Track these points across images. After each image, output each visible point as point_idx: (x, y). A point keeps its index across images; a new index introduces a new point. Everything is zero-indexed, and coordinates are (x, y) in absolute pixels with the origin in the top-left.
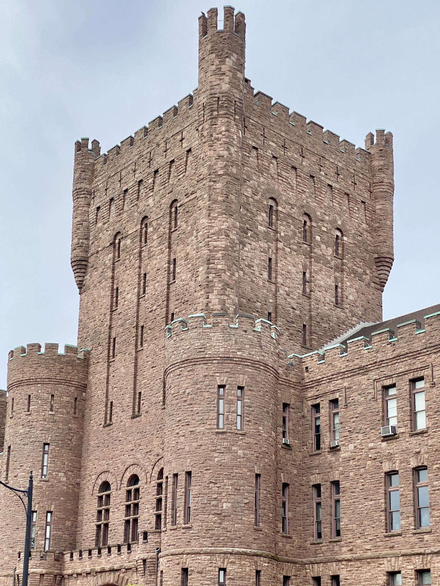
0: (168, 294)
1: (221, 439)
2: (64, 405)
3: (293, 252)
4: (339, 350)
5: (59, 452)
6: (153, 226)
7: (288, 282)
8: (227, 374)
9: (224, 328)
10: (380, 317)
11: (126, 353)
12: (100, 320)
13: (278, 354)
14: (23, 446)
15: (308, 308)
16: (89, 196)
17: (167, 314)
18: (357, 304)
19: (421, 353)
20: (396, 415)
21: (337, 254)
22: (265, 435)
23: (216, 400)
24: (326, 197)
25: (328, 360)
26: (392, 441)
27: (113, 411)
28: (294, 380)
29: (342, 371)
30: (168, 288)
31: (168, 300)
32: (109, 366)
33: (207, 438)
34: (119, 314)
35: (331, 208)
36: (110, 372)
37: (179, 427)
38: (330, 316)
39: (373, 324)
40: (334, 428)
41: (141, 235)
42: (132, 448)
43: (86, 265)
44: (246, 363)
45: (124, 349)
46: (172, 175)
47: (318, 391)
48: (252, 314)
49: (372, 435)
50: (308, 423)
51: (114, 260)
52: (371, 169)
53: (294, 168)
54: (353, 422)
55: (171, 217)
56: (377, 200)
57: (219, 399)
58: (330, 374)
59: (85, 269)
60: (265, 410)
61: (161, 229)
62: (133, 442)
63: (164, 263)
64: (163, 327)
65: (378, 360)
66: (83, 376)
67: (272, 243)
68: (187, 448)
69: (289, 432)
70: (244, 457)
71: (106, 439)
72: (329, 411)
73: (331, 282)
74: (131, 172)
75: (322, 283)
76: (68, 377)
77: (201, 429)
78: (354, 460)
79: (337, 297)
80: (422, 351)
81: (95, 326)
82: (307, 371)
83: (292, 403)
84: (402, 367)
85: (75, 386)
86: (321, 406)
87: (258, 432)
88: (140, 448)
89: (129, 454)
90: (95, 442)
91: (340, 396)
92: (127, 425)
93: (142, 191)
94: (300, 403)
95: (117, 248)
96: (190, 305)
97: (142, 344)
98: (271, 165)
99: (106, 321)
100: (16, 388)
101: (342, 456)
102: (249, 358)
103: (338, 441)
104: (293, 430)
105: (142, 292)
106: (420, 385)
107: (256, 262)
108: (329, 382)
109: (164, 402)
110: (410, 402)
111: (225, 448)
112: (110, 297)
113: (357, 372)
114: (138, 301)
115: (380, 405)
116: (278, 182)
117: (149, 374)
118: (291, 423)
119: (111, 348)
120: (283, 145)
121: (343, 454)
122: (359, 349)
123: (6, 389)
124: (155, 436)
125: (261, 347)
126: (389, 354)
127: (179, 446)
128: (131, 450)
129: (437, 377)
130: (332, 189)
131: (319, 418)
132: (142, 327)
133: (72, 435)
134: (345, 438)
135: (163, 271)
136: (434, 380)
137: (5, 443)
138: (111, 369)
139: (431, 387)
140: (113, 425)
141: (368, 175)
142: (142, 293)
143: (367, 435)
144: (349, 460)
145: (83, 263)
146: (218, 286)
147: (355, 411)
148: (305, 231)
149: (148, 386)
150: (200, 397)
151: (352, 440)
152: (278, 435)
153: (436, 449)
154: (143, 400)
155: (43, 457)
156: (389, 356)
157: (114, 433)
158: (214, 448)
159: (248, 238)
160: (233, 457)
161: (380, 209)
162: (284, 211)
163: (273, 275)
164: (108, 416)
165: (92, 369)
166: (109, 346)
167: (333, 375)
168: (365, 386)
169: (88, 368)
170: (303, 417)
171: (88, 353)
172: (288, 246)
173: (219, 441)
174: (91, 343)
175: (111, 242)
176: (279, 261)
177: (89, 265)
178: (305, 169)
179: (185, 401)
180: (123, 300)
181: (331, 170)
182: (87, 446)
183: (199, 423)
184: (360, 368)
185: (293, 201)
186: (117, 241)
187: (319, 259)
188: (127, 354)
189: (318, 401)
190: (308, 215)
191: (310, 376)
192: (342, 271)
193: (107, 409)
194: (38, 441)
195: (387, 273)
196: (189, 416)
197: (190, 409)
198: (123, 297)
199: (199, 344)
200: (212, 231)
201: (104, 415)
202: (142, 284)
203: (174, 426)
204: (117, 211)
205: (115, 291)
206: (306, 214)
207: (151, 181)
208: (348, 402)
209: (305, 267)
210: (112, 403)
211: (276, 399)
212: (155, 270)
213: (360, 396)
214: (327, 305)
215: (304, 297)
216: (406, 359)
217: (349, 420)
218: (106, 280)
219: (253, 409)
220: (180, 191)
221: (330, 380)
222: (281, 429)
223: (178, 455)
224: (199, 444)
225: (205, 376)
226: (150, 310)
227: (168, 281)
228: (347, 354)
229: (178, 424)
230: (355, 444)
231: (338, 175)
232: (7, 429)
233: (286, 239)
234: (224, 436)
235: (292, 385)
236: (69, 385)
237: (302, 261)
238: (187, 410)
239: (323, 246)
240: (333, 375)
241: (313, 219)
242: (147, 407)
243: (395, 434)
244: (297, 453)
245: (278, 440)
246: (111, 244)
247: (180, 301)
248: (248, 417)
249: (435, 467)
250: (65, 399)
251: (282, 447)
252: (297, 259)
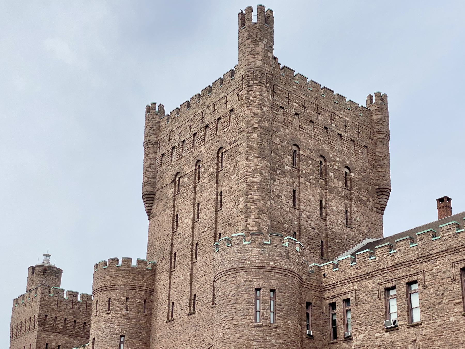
0: (216, 218)
1: (259, 331)
2: (136, 306)
3: (312, 185)
4: (350, 260)
5: (133, 342)
6: (204, 167)
7: (309, 208)
8: (263, 280)
9: (260, 244)
10: (382, 234)
11: (184, 264)
12: (164, 239)
13: (302, 264)
14: (104, 338)
15: (324, 228)
16: (156, 146)
17: (216, 233)
18: (363, 225)
19: (414, 262)
20: (396, 311)
21: (346, 186)
22: (293, 328)
23: (254, 300)
24: (336, 143)
25: (341, 268)
26: (393, 331)
27: (174, 310)
28: (315, 284)
29: (352, 276)
30: (216, 214)
31: (216, 223)
32: (171, 275)
33: (247, 330)
34: (179, 234)
35: (340, 151)
36: (172, 279)
37: (225, 321)
38: (341, 234)
39: (376, 240)
40: (347, 322)
41: (196, 174)
42: (188, 339)
43: (153, 198)
44: (277, 271)
45: (182, 261)
46: (219, 129)
47: (334, 292)
48: (281, 233)
49: (378, 327)
50: (327, 318)
51: (175, 193)
52: (372, 121)
53: (312, 122)
54: (363, 317)
55: (218, 160)
56: (376, 145)
57: (256, 299)
58: (343, 279)
59: (153, 201)
60: (293, 307)
61: (211, 169)
62: (190, 334)
63: (213, 195)
64: (212, 244)
65: (381, 268)
66: (151, 283)
67: (296, 179)
68: (232, 338)
69: (312, 326)
70: (276, 345)
71: (168, 331)
72: (343, 308)
73: (342, 208)
74: (188, 127)
75: (335, 208)
76: (140, 283)
77: (243, 323)
78: (364, 347)
79: (347, 219)
80: (415, 261)
81: (160, 244)
82: (325, 277)
83: (313, 302)
84: (400, 273)
85: (145, 290)
86: (336, 305)
87: (287, 325)
88: (195, 338)
89: (186, 344)
90: (159, 334)
91: (351, 297)
92: (185, 320)
93: (196, 141)
94: (320, 302)
95: (177, 184)
96: (233, 226)
97: (196, 257)
98: (295, 120)
99: (168, 240)
100: (99, 293)
101: (354, 343)
102: (279, 267)
103: (351, 332)
104: (315, 324)
105: (196, 218)
106: (414, 287)
107: (284, 193)
108: (342, 285)
109: (213, 302)
110: (407, 301)
111: (261, 338)
112: (172, 221)
113: (365, 278)
114: (193, 224)
115: (384, 303)
116: (300, 133)
117: (202, 280)
118: (313, 317)
119: (173, 261)
120: (303, 105)
121: (355, 343)
122: (366, 259)
123: (92, 294)
124: (206, 329)
125: (288, 258)
126: (389, 263)
127: (225, 337)
128: (188, 340)
129: (428, 280)
130: (341, 137)
131: (335, 314)
132: (197, 244)
133: (142, 329)
134: (356, 329)
135: (212, 201)
136: (426, 283)
137: (90, 336)
138: (172, 277)
139: (423, 289)
140: (174, 321)
141: (369, 126)
142: (196, 218)
143: (374, 327)
144: (360, 347)
145: (151, 196)
146: (255, 212)
147: (363, 308)
148: (321, 169)
149: (201, 289)
150: (242, 298)
151: (361, 331)
152: (303, 328)
153: (429, 338)
154: (197, 301)
155: (120, 347)
156: (390, 264)
157: (175, 327)
158: (253, 338)
159: (277, 175)
160: (268, 345)
161: (379, 152)
162: (304, 154)
163: (297, 203)
164: (170, 314)
165: (157, 277)
166: (171, 259)
167: (345, 280)
168: (371, 288)
169: (154, 277)
170: (323, 313)
171: (155, 265)
172: (308, 180)
173: (257, 332)
174: (157, 257)
175: (173, 180)
176: (301, 192)
177: (156, 198)
178: (320, 123)
179: (230, 301)
180: (182, 224)
181: (341, 123)
182: (154, 338)
183: (241, 318)
184: (367, 274)
185: (311, 147)
186: (177, 179)
187: (332, 190)
188: (185, 265)
189: (334, 300)
190: (323, 157)
191: (328, 280)
192: (350, 199)
193: (169, 308)
194: (116, 334)
195: (386, 200)
196: (233, 312)
197: (234, 308)
198: (181, 221)
199: (240, 257)
200: (250, 170)
201: (167, 313)
202: (196, 211)
203: (221, 321)
204: (177, 157)
205: (176, 217)
206: (322, 156)
207: (203, 133)
208: (358, 301)
209: (321, 196)
210: (173, 303)
211: (301, 298)
212: (206, 200)
213: (367, 296)
214: (339, 225)
215: (322, 220)
216: (403, 267)
217: (359, 315)
218: (169, 209)
219: (283, 307)
220: (225, 140)
221: (343, 284)
222: (305, 323)
223: (225, 343)
224: (241, 335)
225: (245, 281)
226: (202, 231)
227: (216, 209)
228: (356, 263)
229: (224, 319)
230: (365, 335)
231: (346, 126)
232: (92, 325)
233: (307, 176)
234: (260, 329)
235: (313, 288)
236: (140, 289)
237: (320, 192)
238: (231, 308)
239: (335, 181)
240: (345, 280)
241: (327, 160)
242: (200, 306)
243: (396, 326)
244: (318, 342)
245: (303, 331)
246: (172, 182)
247: (225, 224)
248: (279, 313)
250: (138, 301)
251: (306, 337)
252: (315, 191)
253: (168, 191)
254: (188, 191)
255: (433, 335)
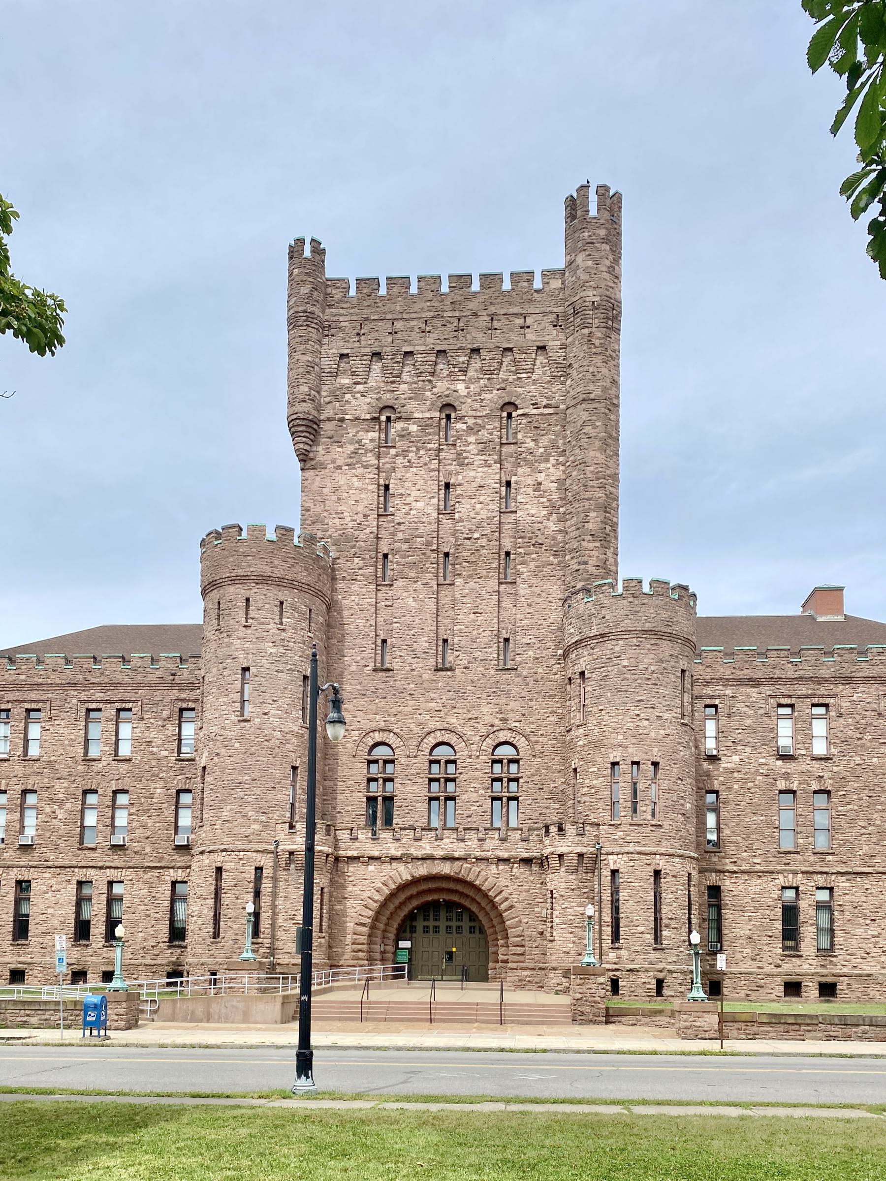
145: (315, 426)
177: (322, 433)
226: (467, 536)
249: (840, 793)
253: (360, 433)
254: (422, 452)
255: (848, 774)
